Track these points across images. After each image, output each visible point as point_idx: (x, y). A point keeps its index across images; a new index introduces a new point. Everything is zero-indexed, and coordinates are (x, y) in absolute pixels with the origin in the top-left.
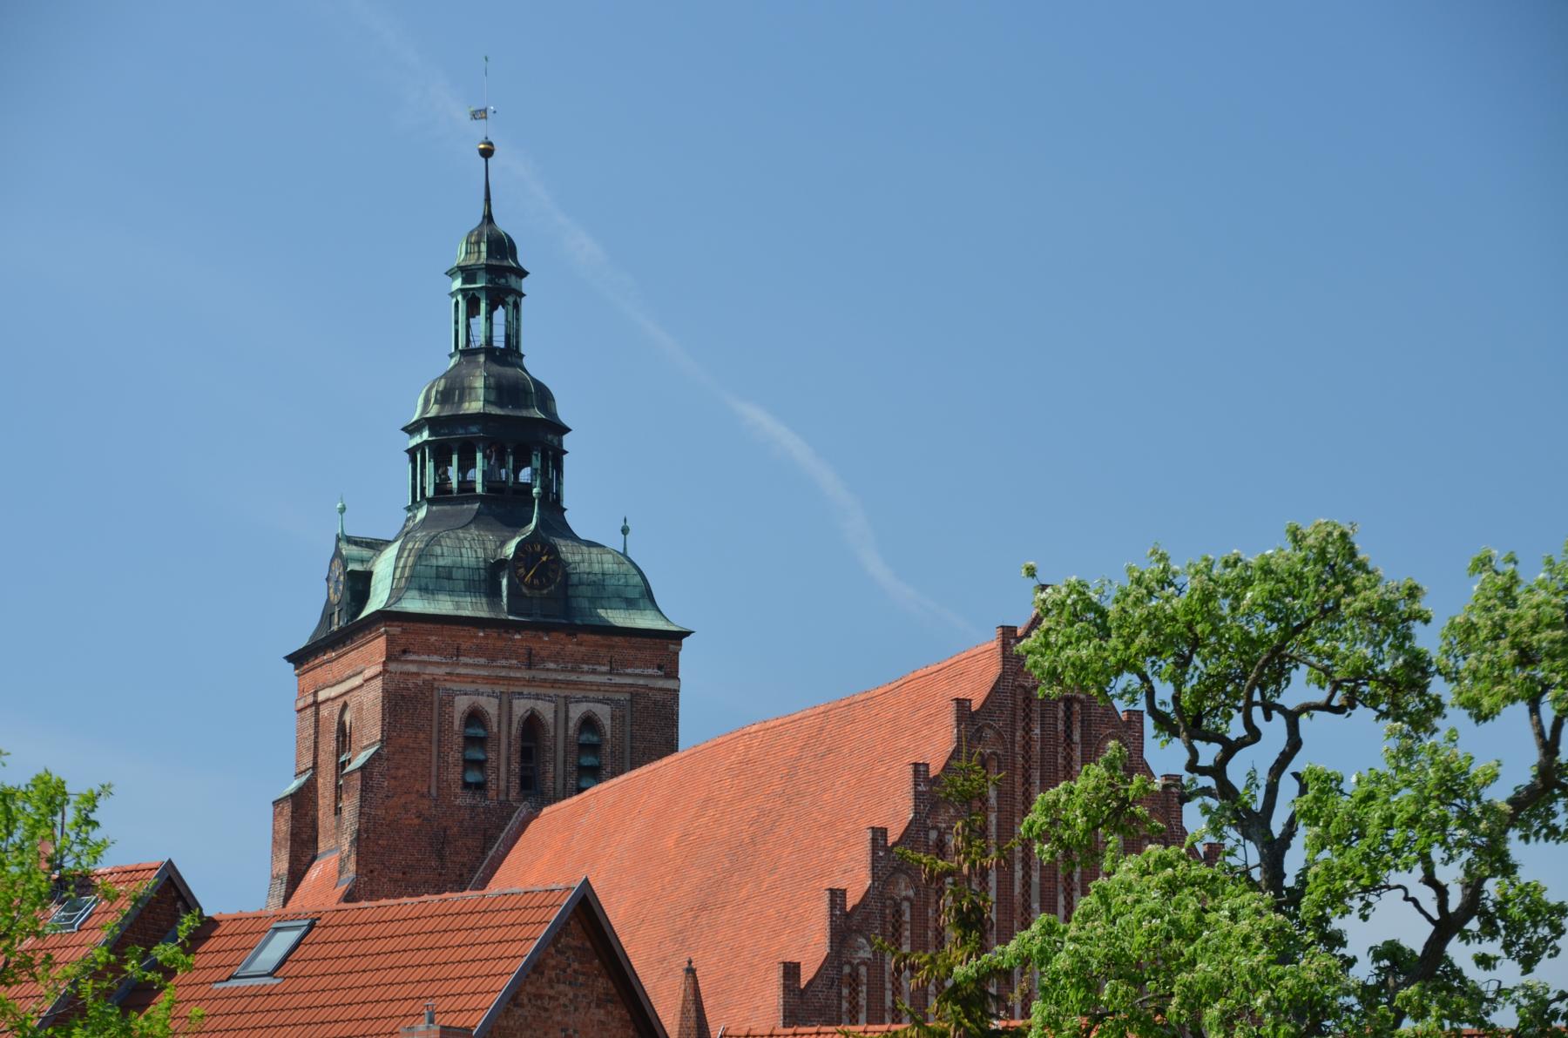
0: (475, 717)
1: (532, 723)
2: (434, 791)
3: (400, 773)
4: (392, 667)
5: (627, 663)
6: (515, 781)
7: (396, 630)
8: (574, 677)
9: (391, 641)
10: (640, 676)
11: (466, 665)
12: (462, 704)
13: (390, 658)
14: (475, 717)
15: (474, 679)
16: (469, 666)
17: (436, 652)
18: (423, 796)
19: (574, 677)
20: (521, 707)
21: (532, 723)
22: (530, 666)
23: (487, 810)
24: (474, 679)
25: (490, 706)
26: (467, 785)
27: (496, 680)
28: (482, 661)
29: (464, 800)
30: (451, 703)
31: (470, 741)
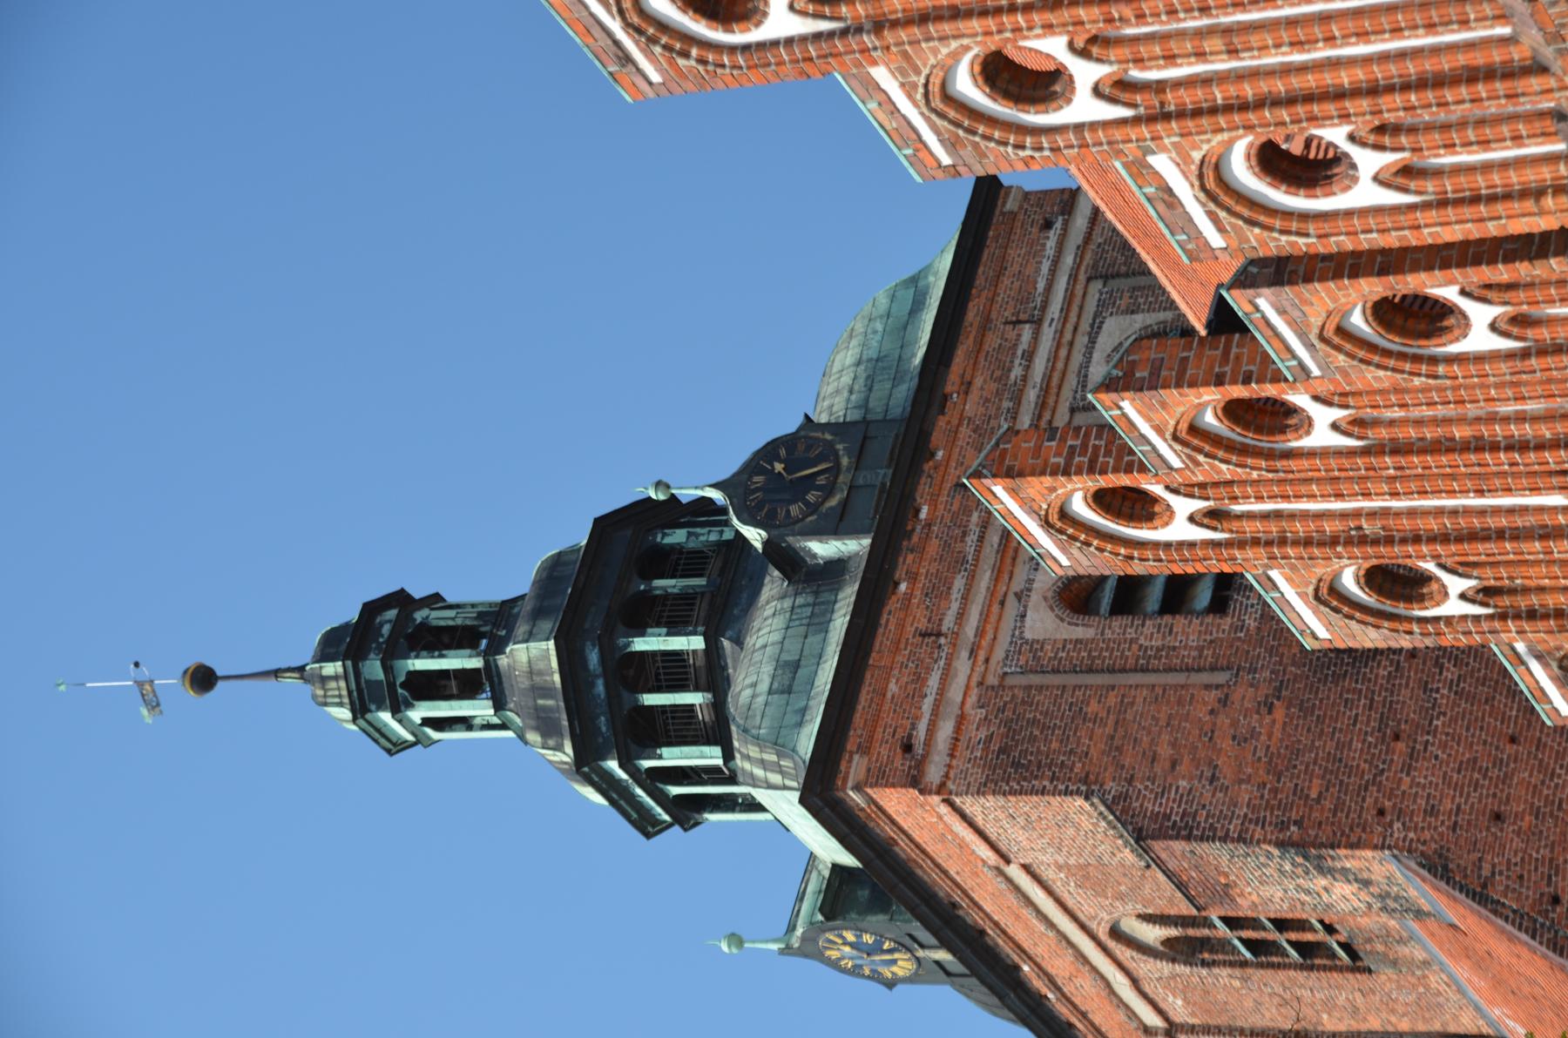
2: (1221, 678)
3: (1165, 751)
8: (1031, 395)
11: (961, 616)
17: (920, 679)
18: (1224, 702)
19: (1031, 395)
28: (959, 583)
30: (1036, 646)
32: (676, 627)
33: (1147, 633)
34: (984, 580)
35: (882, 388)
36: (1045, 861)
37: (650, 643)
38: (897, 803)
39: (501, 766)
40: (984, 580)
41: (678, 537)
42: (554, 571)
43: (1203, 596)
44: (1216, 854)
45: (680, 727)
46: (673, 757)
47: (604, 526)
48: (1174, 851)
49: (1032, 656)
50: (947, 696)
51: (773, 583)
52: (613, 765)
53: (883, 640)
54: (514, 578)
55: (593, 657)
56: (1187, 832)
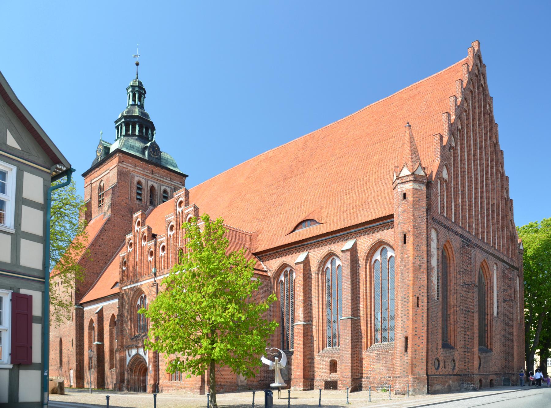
0: (139, 183)
1: (152, 188)
4: (120, 164)
5: (173, 179)
6: (149, 201)
7: (121, 155)
8: (162, 179)
9: (120, 158)
12: (136, 179)
13: (119, 162)
14: (139, 183)
15: (139, 174)
16: (138, 169)
19: (162, 179)
20: (150, 183)
21: (152, 188)
22: (152, 174)
24: (139, 174)
25: (143, 181)
26: (137, 199)
29: (137, 202)
30: (134, 178)
31: (138, 188)
32: (139, 131)
33: (135, 190)
34: (142, 172)
35: (165, 161)
39: (123, 104)
40: (142, 172)
41: (150, 132)
42: (146, 115)
43: (139, 197)
44: (110, 196)
45: (127, 130)
47: (152, 123)
49: (133, 177)
52: (123, 120)
54: (147, 110)
55: (136, 120)
56: (113, 193)
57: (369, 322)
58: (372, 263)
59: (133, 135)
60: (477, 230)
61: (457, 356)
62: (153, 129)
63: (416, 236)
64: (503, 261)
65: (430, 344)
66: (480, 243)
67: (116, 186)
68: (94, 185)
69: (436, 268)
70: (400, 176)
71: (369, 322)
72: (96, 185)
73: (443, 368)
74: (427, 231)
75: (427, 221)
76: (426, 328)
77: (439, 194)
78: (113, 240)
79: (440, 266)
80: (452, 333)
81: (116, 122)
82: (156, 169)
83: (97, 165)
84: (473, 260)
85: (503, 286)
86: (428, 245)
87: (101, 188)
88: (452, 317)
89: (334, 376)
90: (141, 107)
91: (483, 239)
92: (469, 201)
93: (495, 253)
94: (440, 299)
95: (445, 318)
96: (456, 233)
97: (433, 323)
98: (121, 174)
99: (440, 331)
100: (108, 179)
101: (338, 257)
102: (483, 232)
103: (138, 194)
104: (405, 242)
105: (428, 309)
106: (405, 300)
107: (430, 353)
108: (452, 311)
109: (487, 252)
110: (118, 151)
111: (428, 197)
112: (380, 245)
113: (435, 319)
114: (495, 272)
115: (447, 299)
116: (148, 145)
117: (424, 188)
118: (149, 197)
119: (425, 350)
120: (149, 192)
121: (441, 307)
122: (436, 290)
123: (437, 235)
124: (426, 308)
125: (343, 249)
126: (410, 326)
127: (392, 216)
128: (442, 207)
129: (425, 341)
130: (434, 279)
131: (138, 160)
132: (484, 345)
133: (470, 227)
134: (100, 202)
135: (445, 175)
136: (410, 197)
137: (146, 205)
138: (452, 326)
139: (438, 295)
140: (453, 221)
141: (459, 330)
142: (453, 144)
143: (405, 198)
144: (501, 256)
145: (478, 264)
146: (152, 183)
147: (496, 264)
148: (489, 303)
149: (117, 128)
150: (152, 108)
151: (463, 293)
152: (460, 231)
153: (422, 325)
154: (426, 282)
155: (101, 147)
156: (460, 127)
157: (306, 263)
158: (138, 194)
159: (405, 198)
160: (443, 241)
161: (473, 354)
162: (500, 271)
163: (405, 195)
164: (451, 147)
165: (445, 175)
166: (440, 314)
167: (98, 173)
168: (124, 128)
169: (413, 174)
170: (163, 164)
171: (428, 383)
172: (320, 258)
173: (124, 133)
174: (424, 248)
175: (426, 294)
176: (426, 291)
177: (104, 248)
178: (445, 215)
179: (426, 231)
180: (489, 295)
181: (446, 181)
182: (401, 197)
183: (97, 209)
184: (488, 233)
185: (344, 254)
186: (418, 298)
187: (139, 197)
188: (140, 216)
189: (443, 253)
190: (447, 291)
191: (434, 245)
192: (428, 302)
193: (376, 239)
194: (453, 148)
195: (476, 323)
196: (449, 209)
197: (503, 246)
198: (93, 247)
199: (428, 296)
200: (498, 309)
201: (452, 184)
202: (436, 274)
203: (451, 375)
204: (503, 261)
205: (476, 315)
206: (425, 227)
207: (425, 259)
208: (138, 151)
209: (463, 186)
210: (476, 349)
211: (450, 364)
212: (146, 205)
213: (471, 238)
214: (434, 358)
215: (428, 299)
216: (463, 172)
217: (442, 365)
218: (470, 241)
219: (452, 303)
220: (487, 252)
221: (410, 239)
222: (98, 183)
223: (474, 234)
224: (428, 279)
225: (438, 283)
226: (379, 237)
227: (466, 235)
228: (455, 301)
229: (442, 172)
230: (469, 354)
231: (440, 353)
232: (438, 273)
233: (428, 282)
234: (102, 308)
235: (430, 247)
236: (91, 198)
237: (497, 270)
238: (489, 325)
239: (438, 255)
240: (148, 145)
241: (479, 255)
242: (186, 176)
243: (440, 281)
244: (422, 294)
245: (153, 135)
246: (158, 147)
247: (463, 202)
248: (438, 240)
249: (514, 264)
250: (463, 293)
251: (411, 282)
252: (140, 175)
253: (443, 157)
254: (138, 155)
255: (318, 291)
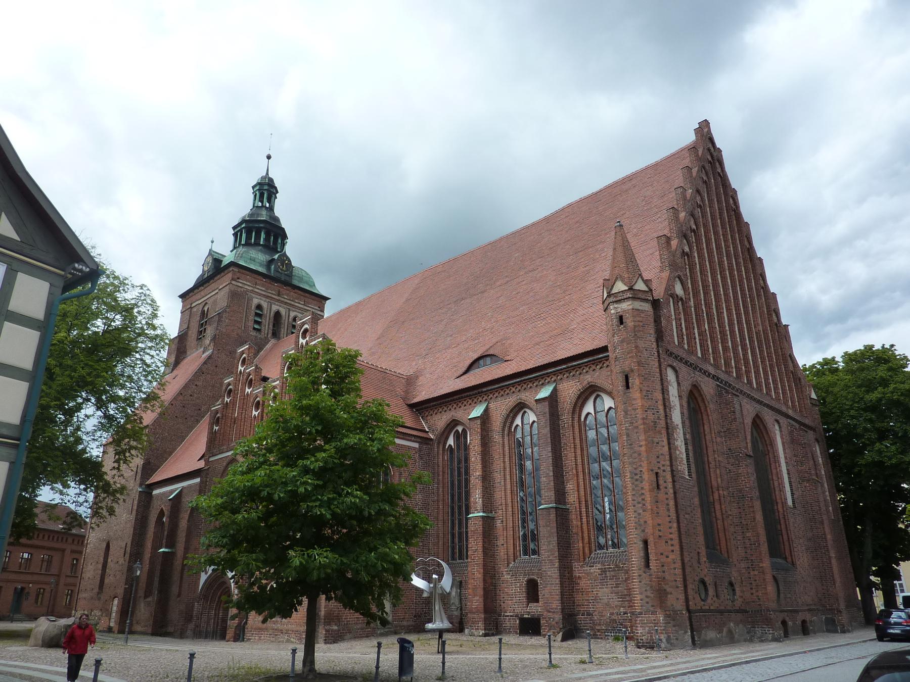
0: (259, 307)
1: (278, 315)
4: (233, 282)
6: (270, 332)
7: (236, 270)
9: (234, 274)
10: (313, 307)
12: (256, 301)
13: (233, 279)
14: (259, 307)
15: (260, 295)
16: (260, 289)
20: (275, 308)
21: (278, 315)
22: (279, 295)
23: (261, 339)
24: (260, 295)
25: (265, 305)
26: (254, 329)
27: (267, 297)
29: (253, 333)
31: (257, 315)
32: (265, 240)
33: (252, 317)
36: (219, 296)
37: (263, 235)
38: (230, 275)
41: (280, 241)
43: (256, 326)
44: (215, 325)
45: (248, 238)
46: (244, 235)
48: (216, 319)
50: (245, 284)
51: (269, 258)
53: (256, 276)
54: (277, 212)
55: (262, 225)
56: (219, 321)
57: (584, 514)
58: (582, 419)
59: (257, 244)
60: (738, 369)
61: (735, 576)
62: (284, 236)
63: (645, 378)
64: (787, 416)
65: (685, 553)
66: (746, 389)
67: (225, 311)
68: (195, 310)
69: (680, 426)
70: (613, 292)
71: (584, 514)
72: (197, 310)
73: (715, 599)
74: (660, 370)
75: (659, 356)
76: (675, 525)
77: (673, 317)
78: (213, 386)
79: (687, 422)
80: (722, 535)
81: (234, 228)
82: (284, 290)
83: (202, 283)
84: (738, 415)
85: (795, 456)
86: (664, 391)
87: (203, 314)
88: (717, 507)
89: (535, 609)
90: (271, 209)
91: (750, 382)
92: (720, 327)
93: (773, 404)
94: (694, 475)
95: (707, 507)
96: (706, 373)
97: (687, 516)
98: (235, 296)
99: (700, 530)
100: (215, 302)
101: (531, 409)
102: (748, 372)
103: (256, 322)
104: (628, 387)
105: (675, 493)
106: (637, 477)
107: (688, 570)
108: (716, 496)
109: (760, 402)
110: (232, 264)
111: (657, 320)
112: (591, 391)
113: (689, 509)
114: (778, 432)
115: (705, 476)
116: (276, 257)
117: (647, 307)
118: (271, 326)
119: (679, 564)
120: (272, 320)
121: (696, 489)
122: (685, 462)
123: (677, 377)
124: (671, 491)
125: (537, 398)
126: (650, 522)
127: (605, 349)
128: (681, 336)
129: (677, 548)
130: (680, 443)
131: (260, 277)
132: (780, 557)
133: (727, 364)
134: (201, 333)
135: (679, 290)
136: (629, 322)
137: (266, 338)
138: (720, 522)
139: (689, 469)
140: (700, 355)
141: (732, 529)
142: (687, 249)
143: (622, 323)
144: (784, 409)
145: (748, 421)
146: (278, 307)
147: (777, 421)
148: (776, 483)
149: (235, 235)
150: (282, 209)
151: (729, 466)
152: (711, 370)
153: (668, 519)
154: (666, 448)
155: (210, 260)
156: (694, 227)
157: (485, 418)
158: (256, 322)
159: (622, 323)
160: (686, 386)
161: (763, 573)
162: (785, 432)
163: (621, 318)
164: (684, 254)
165: (679, 290)
166: (696, 501)
167: (202, 293)
168: (244, 235)
169: (631, 289)
170: (295, 282)
171: (691, 625)
172: (505, 412)
173: (243, 242)
174: (659, 396)
175: (669, 469)
176: (668, 463)
177: (198, 398)
178: (686, 346)
179: (658, 370)
180: (774, 471)
181: (681, 299)
182: (616, 321)
183: (196, 343)
184: (757, 373)
185: (539, 406)
186: (657, 473)
187: (256, 326)
188: (246, 351)
189: (689, 403)
190: (703, 463)
191: (673, 391)
192: (674, 481)
193: (586, 382)
194: (687, 254)
195: (759, 517)
196: (691, 337)
197: (784, 393)
198: (181, 398)
199: (672, 471)
200: (792, 494)
201: (692, 303)
202: (681, 435)
203: (730, 611)
204: (787, 416)
205: (758, 505)
206: (657, 364)
207: (662, 411)
208: (261, 265)
209: (708, 305)
210: (766, 563)
211: (725, 591)
212: (266, 338)
213: (731, 380)
214: (697, 579)
215: (673, 476)
216: (705, 287)
217: (711, 592)
218: (730, 385)
219: (714, 483)
220: (760, 402)
221: (635, 381)
222: (201, 306)
223: (735, 374)
224: (669, 444)
225: (687, 450)
226: (590, 380)
227: (722, 376)
228: (719, 480)
229: (674, 287)
230: (756, 573)
231: (706, 571)
232: (685, 434)
233: (670, 449)
234: (179, 495)
235: (668, 395)
236: (188, 327)
237: (781, 431)
238: (782, 521)
239: (681, 406)
240: (276, 257)
241: (748, 406)
242: (327, 299)
243: (690, 448)
244: (662, 468)
245: (283, 245)
246: (289, 261)
247: (711, 328)
248: (679, 384)
249: (807, 421)
250: (729, 466)
251: (643, 448)
252: (260, 297)
253: (673, 266)
254: (261, 269)
255: (504, 462)
